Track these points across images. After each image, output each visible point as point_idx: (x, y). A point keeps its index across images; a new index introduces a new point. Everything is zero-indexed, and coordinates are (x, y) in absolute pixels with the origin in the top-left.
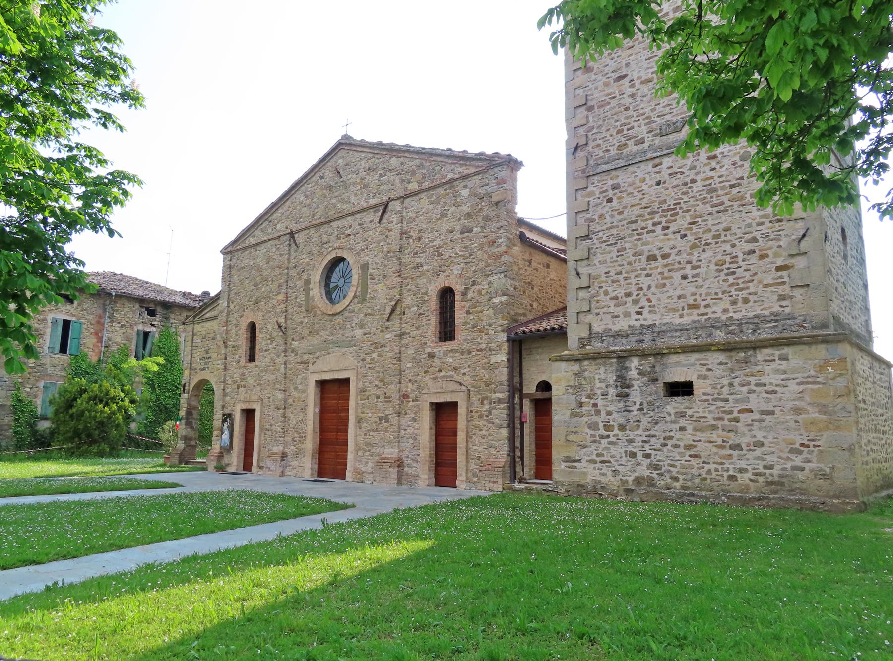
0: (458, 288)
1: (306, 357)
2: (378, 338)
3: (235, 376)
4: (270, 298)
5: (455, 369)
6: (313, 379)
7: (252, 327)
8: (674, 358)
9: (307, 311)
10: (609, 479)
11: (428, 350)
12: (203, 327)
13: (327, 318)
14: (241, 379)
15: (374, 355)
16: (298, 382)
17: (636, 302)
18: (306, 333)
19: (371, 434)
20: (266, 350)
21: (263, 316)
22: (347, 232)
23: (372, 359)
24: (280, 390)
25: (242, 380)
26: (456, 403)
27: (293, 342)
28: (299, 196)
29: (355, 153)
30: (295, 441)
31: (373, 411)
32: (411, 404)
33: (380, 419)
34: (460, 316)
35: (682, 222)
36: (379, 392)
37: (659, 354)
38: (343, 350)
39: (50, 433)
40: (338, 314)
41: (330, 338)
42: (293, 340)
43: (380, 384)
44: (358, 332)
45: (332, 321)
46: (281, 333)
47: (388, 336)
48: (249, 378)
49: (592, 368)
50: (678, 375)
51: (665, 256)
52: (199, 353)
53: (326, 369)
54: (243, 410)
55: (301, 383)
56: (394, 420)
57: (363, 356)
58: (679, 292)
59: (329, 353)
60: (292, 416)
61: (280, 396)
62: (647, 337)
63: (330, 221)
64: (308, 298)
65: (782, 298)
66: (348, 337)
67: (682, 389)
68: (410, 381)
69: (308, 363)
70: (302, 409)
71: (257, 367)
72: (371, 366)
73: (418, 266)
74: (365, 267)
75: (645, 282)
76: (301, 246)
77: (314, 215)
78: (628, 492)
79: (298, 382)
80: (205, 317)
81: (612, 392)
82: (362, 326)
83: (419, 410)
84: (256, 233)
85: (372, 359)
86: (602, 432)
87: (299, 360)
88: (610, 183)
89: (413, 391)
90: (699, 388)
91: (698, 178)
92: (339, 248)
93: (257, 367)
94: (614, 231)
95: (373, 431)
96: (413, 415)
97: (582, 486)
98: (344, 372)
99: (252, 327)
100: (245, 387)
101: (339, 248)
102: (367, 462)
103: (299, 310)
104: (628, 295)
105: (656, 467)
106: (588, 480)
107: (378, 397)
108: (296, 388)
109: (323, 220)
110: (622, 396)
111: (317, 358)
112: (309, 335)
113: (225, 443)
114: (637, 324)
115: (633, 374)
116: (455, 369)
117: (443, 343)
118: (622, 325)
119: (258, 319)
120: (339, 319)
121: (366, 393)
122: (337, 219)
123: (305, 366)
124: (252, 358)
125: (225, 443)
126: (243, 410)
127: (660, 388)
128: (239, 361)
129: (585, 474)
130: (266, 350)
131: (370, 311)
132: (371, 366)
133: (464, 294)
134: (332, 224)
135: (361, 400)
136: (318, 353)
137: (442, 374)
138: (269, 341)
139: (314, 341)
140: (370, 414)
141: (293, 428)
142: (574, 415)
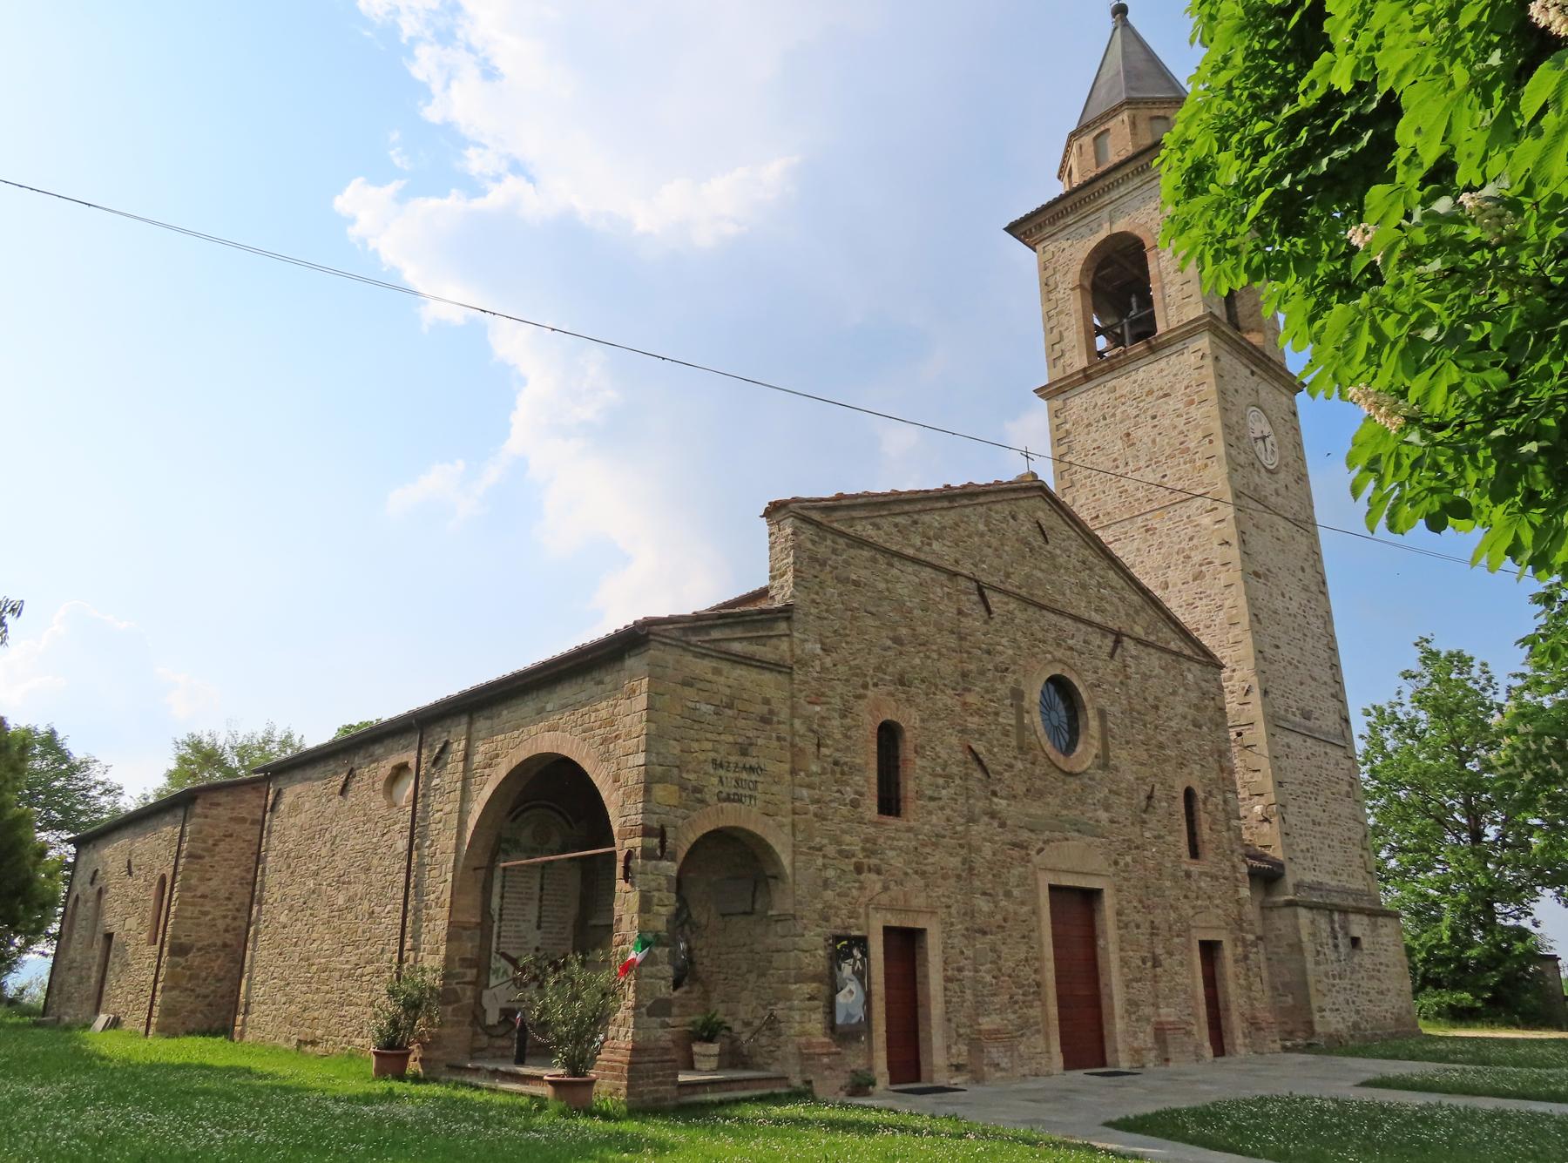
0: (1201, 795)
1: (1025, 835)
2: (1133, 832)
3: (847, 838)
4: (936, 686)
5: (1209, 897)
6: (1047, 880)
7: (889, 734)
8: (1352, 917)
9: (1020, 748)
10: (1341, 1026)
11: (1185, 867)
12: (717, 671)
13: (1057, 774)
14: (864, 849)
15: (1128, 859)
16: (1013, 881)
17: (1312, 859)
18: (1021, 789)
19: (1135, 984)
20: (932, 799)
21: (923, 720)
22: (1070, 642)
23: (1127, 865)
24: (984, 894)
25: (870, 853)
26: (1220, 942)
27: (995, 800)
28: (975, 517)
29: (1061, 522)
30: (1016, 1002)
31: (1135, 948)
32: (1176, 940)
33: (1144, 962)
34: (1205, 832)
35: (1321, 800)
36: (1138, 918)
37: (1344, 911)
38: (1089, 839)
39: (390, 1024)
40: (1077, 774)
41: (1064, 812)
42: (994, 794)
43: (1140, 906)
44: (1103, 816)
45: (1064, 783)
46: (978, 774)
47: (1147, 834)
48: (891, 853)
49: (1317, 918)
50: (1356, 931)
51: (1319, 824)
52: (709, 745)
53: (1064, 867)
54: (888, 931)
55: (1018, 886)
56: (1167, 962)
57: (1114, 856)
58: (1329, 858)
59: (1067, 839)
60: (1005, 950)
61: (983, 905)
62: (1324, 893)
63: (1042, 607)
64: (1021, 727)
65: (1364, 879)
66: (1090, 818)
67: (1355, 942)
68: (1171, 906)
69: (1026, 848)
70: (1024, 937)
71: (909, 830)
72: (1126, 875)
73: (1161, 746)
74: (1102, 714)
75: (1315, 843)
76: (998, 620)
77: (1008, 575)
78: (1352, 1036)
79: (1013, 881)
80: (725, 646)
81: (1330, 941)
82: (1107, 808)
83: (1188, 947)
84: (886, 524)
85: (1127, 865)
86: (1332, 981)
87: (1009, 837)
88: (1286, 740)
89: (1176, 922)
90: (1365, 943)
91: (1324, 765)
92: (1065, 663)
93: (909, 830)
94: (1293, 787)
95: (1138, 980)
96: (1179, 957)
97: (1331, 1035)
98: (1094, 878)
99: (889, 734)
100: (879, 872)
101: (1065, 663)
102: (1135, 1033)
103: (1004, 740)
104: (1308, 850)
105: (1357, 1012)
106: (1332, 1030)
107: (1138, 927)
108: (1008, 894)
109: (1023, 592)
110: (1336, 946)
111: (1045, 842)
112: (1025, 795)
113: (849, 1016)
114: (1315, 879)
115: (1337, 926)
116: (1209, 897)
117: (1194, 861)
118: (1309, 878)
119: (909, 720)
120: (1074, 784)
121: (1124, 918)
122: (1054, 611)
123: (1023, 852)
124: (890, 803)
125: (849, 1016)
126: (888, 931)
127: (1348, 941)
128: (855, 804)
129: (1329, 1023)
130: (932, 799)
131: (1114, 788)
132: (1126, 875)
133: (1205, 804)
134: (1045, 612)
135: (1119, 928)
136: (1047, 833)
137: (1199, 902)
138: (941, 781)
139: (1036, 809)
140: (1131, 954)
141: (1010, 976)
142: (1317, 963)
